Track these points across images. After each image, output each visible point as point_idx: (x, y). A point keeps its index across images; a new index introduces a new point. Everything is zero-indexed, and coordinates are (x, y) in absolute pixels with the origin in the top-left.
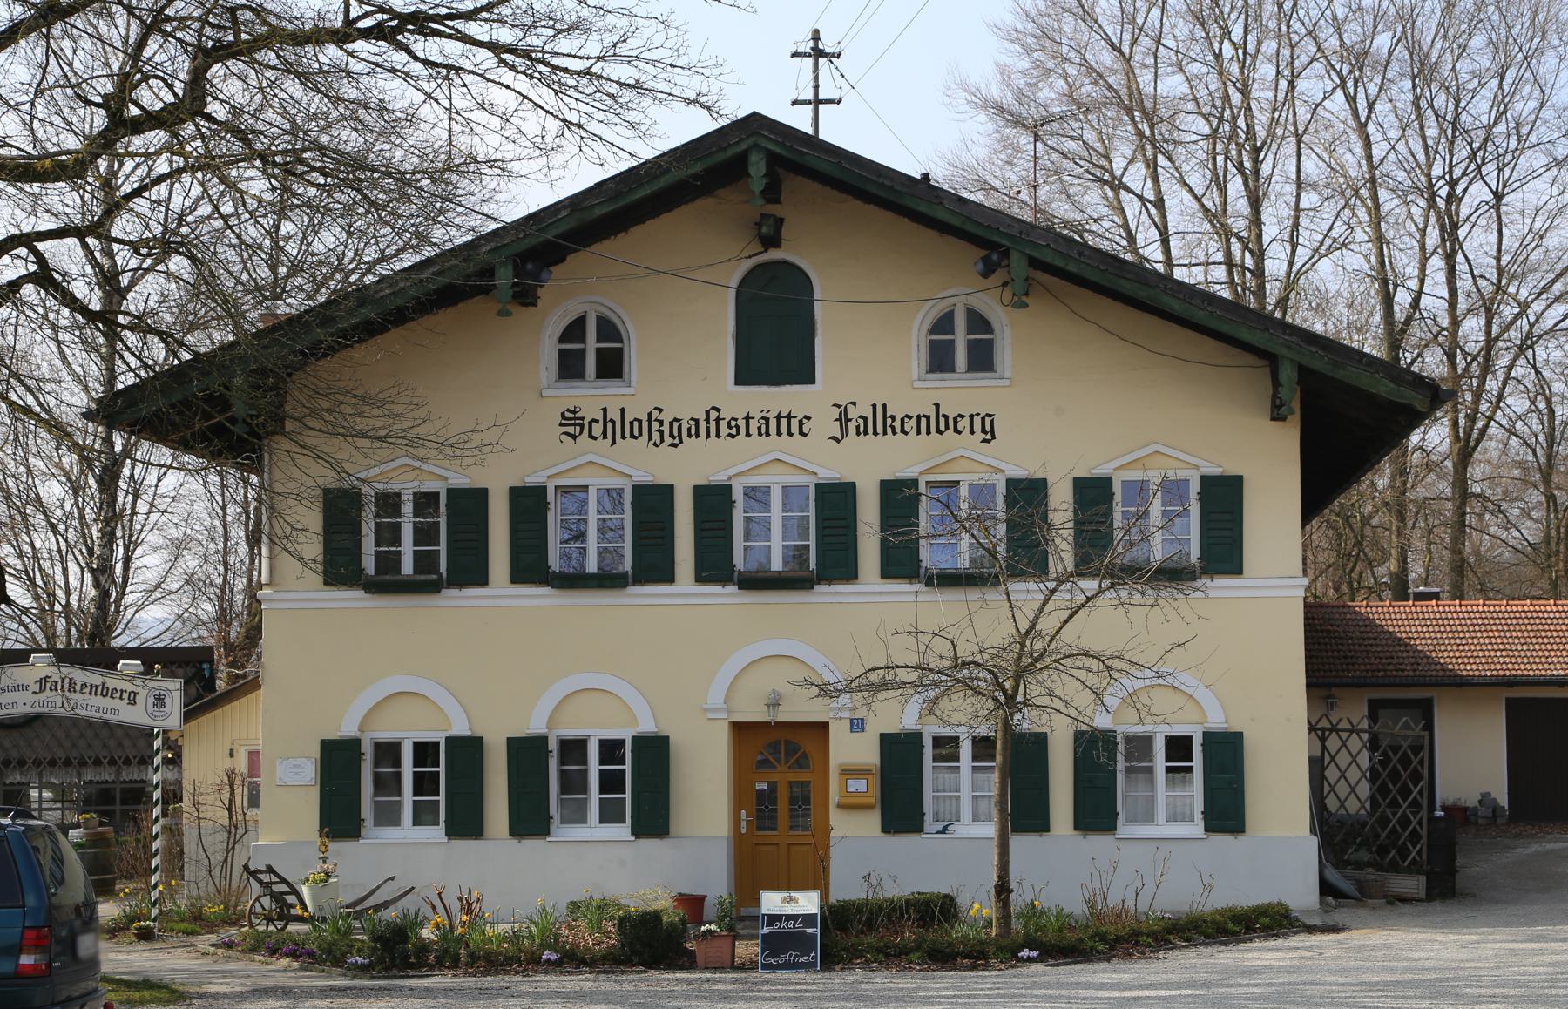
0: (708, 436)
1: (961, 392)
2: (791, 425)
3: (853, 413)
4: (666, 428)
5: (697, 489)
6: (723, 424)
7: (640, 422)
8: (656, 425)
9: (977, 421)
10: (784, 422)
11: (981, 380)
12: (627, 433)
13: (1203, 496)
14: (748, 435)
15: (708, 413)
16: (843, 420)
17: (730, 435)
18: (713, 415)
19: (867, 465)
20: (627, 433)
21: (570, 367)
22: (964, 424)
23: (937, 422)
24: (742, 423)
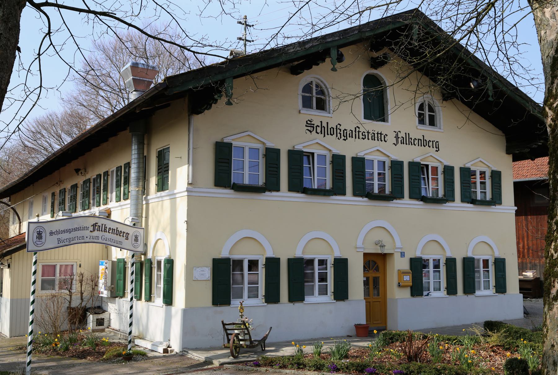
0: (356, 138)
1: (428, 132)
2: (380, 137)
3: (400, 136)
4: (342, 132)
5: (409, 162)
6: (360, 134)
7: (333, 129)
8: (338, 131)
9: (434, 143)
10: (379, 135)
11: (431, 128)
12: (329, 133)
13: (332, 162)
14: (368, 139)
15: (337, 126)
16: (397, 137)
17: (363, 138)
18: (357, 129)
19: (407, 154)
20: (329, 133)
21: (307, 103)
22: (431, 144)
23: (423, 142)
24: (366, 134)
